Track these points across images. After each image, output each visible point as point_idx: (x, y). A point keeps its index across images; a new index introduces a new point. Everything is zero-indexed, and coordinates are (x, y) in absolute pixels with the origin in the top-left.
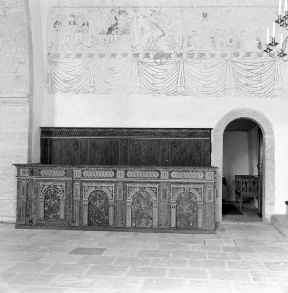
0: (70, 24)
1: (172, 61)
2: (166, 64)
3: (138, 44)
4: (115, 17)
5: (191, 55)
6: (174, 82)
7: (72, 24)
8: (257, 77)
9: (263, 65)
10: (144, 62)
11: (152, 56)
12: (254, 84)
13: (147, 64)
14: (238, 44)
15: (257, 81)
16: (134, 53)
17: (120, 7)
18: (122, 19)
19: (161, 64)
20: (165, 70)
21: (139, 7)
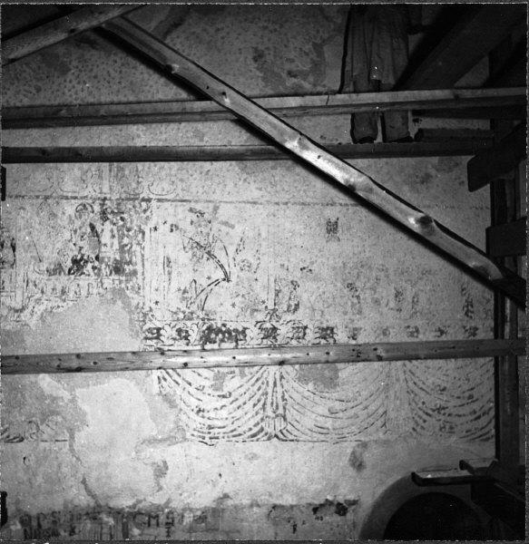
3: (157, 303)
4: (93, 227)
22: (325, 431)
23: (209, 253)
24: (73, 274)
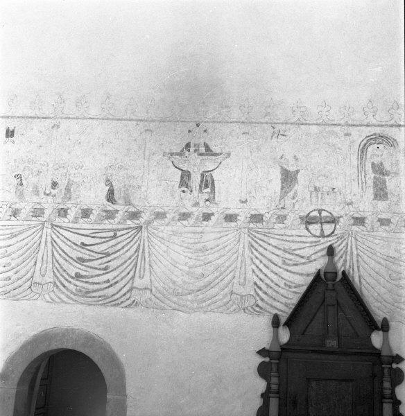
8: (100, 261)
9: (115, 237)
12: (92, 277)
14: (68, 189)
15: (100, 269)
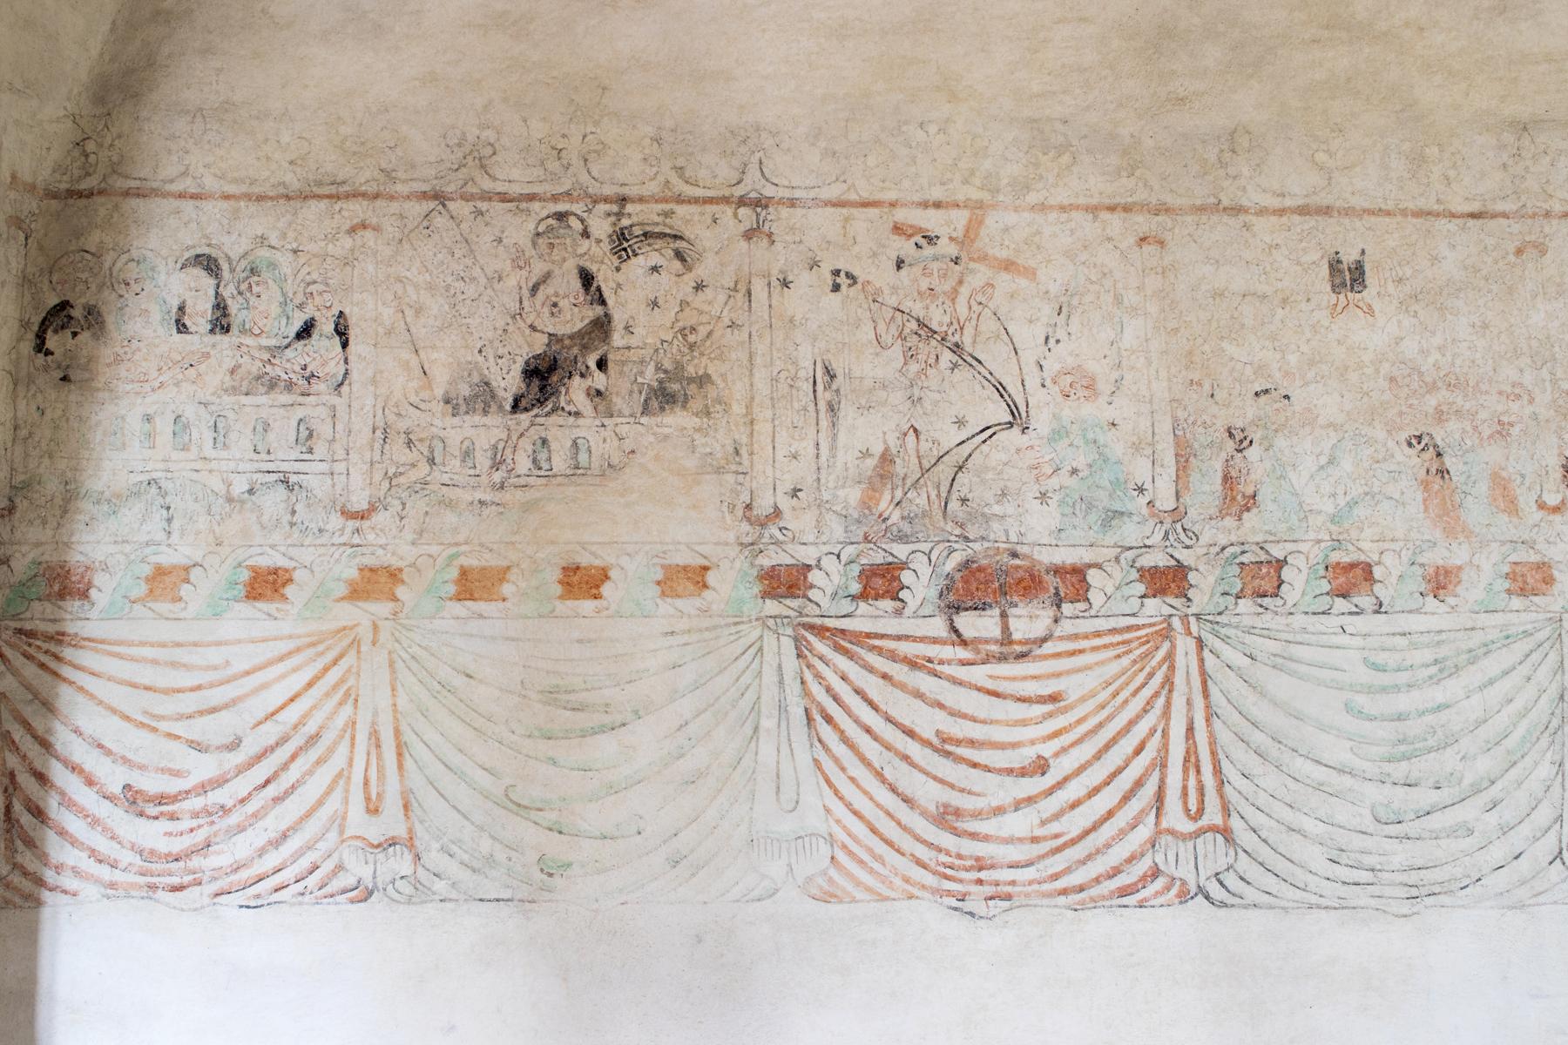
0: (181, 327)
1: (1102, 624)
2: (1049, 648)
3: (795, 492)
4: (587, 279)
5: (1263, 579)
6: (1126, 798)
7: (200, 319)
10: (860, 638)
11: (921, 586)
13: (893, 656)
16: (766, 562)
17: (623, 200)
18: (635, 289)
19: (1011, 650)
20: (1042, 700)
21: (792, 203)
22: (1365, 876)
23: (957, 348)
24: (526, 410)
